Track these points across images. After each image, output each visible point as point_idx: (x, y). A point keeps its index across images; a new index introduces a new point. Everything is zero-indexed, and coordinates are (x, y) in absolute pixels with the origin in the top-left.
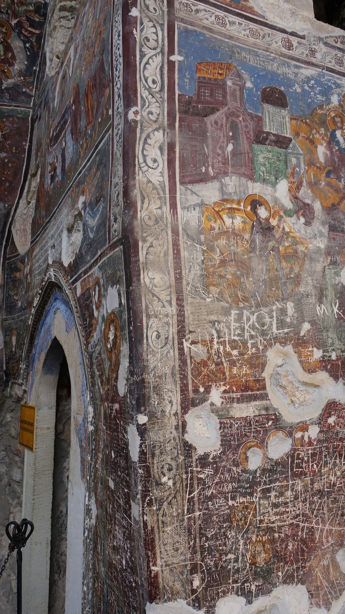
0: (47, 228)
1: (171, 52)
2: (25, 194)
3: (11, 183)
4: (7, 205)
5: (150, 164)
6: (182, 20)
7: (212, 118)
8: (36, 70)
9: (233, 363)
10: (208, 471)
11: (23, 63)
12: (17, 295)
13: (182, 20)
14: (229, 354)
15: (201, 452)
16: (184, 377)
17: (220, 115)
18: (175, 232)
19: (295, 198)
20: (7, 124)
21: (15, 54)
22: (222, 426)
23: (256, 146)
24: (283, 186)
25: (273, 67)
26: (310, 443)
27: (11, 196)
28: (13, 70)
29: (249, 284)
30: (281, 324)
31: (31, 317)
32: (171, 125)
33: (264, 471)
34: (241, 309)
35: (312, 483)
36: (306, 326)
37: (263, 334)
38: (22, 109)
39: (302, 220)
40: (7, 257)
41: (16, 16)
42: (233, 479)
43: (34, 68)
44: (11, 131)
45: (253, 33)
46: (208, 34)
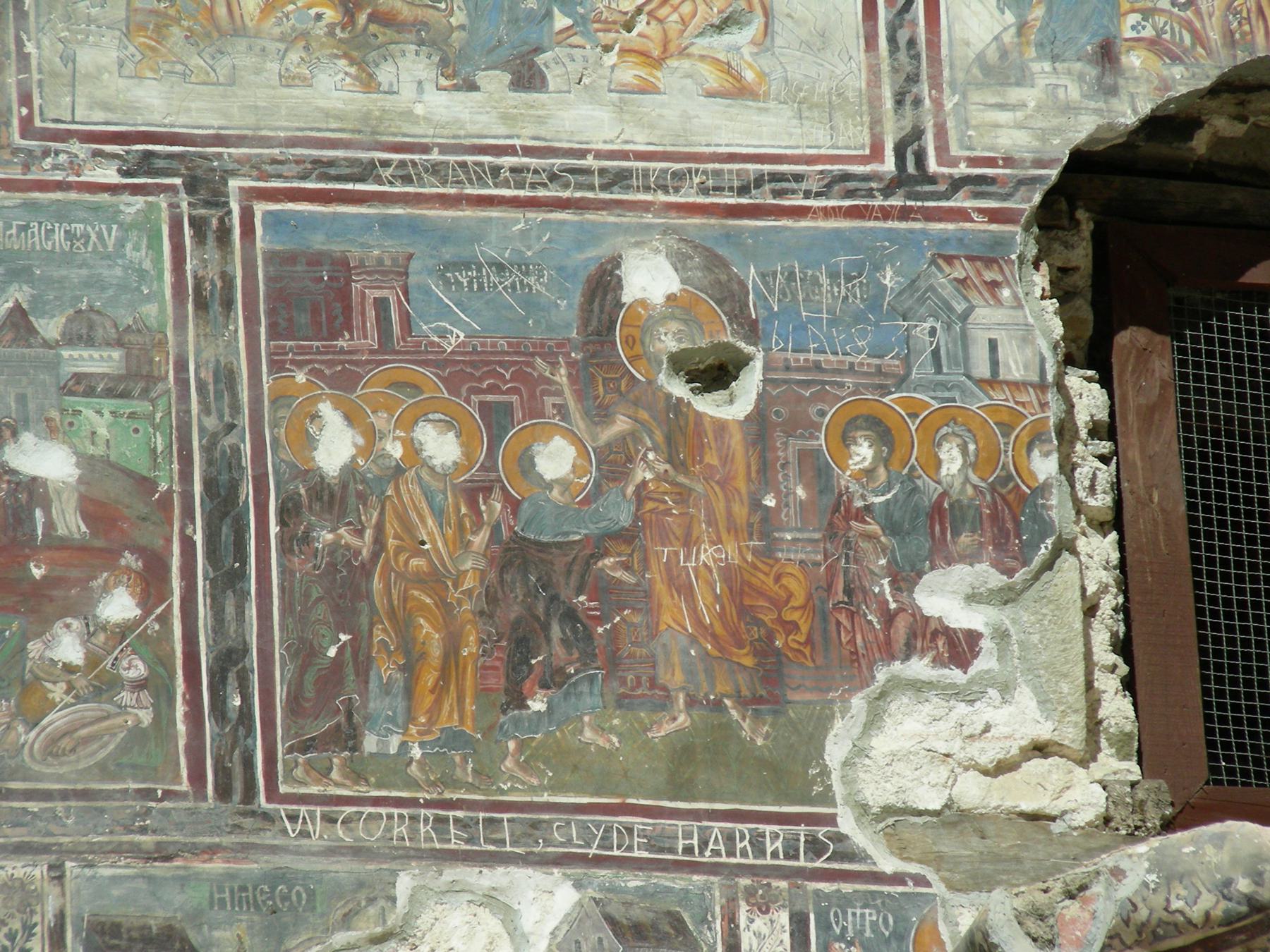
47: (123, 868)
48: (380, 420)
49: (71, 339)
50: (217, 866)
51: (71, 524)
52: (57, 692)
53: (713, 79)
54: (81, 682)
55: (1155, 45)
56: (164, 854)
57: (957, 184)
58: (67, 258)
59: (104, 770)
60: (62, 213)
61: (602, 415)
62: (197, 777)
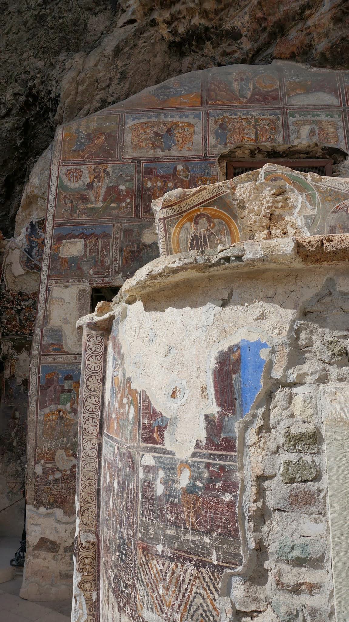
1: (39, 374)
5: (32, 405)
6: (42, 363)
7: (49, 389)
9: (47, 454)
10: (39, 479)
13: (42, 363)
14: (46, 452)
15: (38, 474)
16: (35, 457)
17: (51, 388)
18: (37, 422)
19: (71, 407)
22: (43, 469)
23: (61, 394)
24: (68, 405)
25: (69, 368)
26: (67, 475)
29: (54, 434)
30: (62, 444)
32: (38, 394)
33: (53, 480)
34: (51, 441)
35: (68, 485)
36: (69, 444)
37: (56, 447)
39: (73, 414)
42: (45, 481)
45: (64, 359)
46: (49, 365)
47: (127, 224)
48: (154, 182)
49: (126, 176)
50: (136, 223)
51: (124, 193)
52: (122, 208)
53: (187, 149)
54: (125, 207)
55: (230, 143)
56: (131, 223)
57: (210, 157)
58: (125, 169)
59: (126, 215)
60: (126, 165)
61: (175, 180)
62: (135, 215)
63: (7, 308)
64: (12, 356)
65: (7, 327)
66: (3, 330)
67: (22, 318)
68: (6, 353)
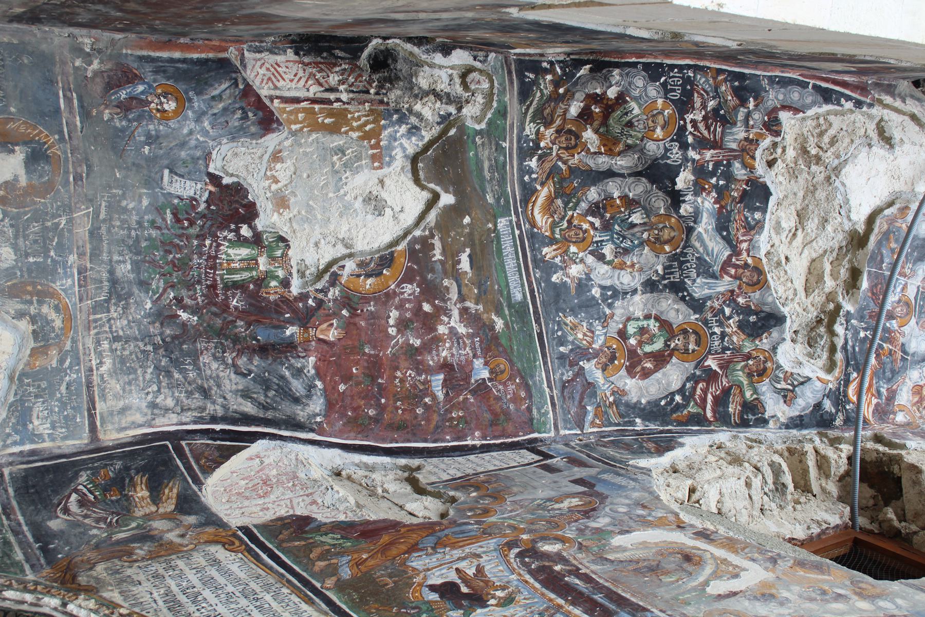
0: (310, 602)
2: (357, 458)
3: (376, 420)
4: (318, 419)
8: (633, 423)
11: (642, 396)
12: (82, 503)
20: (511, 387)
21: (653, 377)
27: (344, 425)
28: (621, 377)
31: (29, 597)
38: (551, 415)
40: (183, 443)
41: (725, 365)
43: (638, 420)
44: (498, 399)
63: (684, 105)
64: (402, 120)
65: (569, 96)
66: (552, 71)
67: (614, 189)
68: (423, 82)
